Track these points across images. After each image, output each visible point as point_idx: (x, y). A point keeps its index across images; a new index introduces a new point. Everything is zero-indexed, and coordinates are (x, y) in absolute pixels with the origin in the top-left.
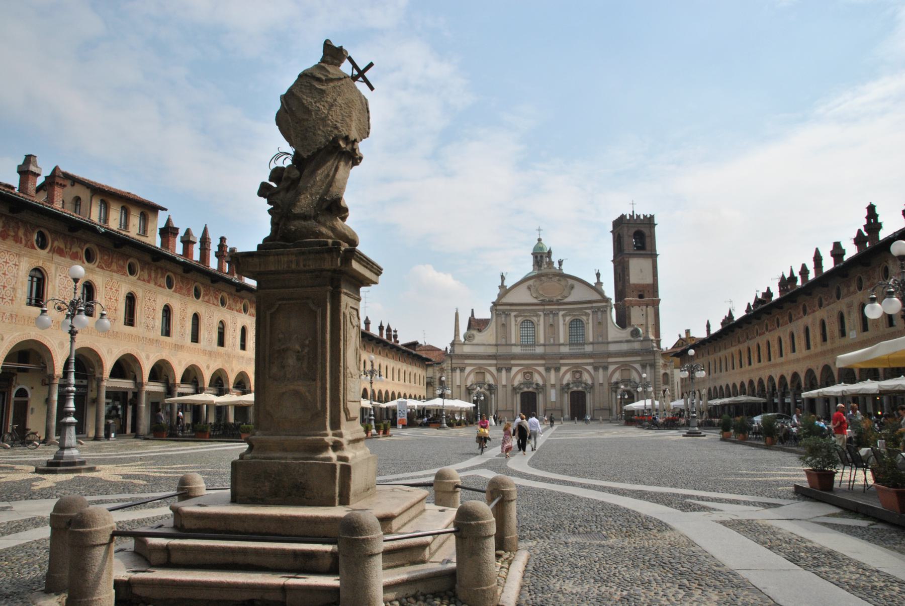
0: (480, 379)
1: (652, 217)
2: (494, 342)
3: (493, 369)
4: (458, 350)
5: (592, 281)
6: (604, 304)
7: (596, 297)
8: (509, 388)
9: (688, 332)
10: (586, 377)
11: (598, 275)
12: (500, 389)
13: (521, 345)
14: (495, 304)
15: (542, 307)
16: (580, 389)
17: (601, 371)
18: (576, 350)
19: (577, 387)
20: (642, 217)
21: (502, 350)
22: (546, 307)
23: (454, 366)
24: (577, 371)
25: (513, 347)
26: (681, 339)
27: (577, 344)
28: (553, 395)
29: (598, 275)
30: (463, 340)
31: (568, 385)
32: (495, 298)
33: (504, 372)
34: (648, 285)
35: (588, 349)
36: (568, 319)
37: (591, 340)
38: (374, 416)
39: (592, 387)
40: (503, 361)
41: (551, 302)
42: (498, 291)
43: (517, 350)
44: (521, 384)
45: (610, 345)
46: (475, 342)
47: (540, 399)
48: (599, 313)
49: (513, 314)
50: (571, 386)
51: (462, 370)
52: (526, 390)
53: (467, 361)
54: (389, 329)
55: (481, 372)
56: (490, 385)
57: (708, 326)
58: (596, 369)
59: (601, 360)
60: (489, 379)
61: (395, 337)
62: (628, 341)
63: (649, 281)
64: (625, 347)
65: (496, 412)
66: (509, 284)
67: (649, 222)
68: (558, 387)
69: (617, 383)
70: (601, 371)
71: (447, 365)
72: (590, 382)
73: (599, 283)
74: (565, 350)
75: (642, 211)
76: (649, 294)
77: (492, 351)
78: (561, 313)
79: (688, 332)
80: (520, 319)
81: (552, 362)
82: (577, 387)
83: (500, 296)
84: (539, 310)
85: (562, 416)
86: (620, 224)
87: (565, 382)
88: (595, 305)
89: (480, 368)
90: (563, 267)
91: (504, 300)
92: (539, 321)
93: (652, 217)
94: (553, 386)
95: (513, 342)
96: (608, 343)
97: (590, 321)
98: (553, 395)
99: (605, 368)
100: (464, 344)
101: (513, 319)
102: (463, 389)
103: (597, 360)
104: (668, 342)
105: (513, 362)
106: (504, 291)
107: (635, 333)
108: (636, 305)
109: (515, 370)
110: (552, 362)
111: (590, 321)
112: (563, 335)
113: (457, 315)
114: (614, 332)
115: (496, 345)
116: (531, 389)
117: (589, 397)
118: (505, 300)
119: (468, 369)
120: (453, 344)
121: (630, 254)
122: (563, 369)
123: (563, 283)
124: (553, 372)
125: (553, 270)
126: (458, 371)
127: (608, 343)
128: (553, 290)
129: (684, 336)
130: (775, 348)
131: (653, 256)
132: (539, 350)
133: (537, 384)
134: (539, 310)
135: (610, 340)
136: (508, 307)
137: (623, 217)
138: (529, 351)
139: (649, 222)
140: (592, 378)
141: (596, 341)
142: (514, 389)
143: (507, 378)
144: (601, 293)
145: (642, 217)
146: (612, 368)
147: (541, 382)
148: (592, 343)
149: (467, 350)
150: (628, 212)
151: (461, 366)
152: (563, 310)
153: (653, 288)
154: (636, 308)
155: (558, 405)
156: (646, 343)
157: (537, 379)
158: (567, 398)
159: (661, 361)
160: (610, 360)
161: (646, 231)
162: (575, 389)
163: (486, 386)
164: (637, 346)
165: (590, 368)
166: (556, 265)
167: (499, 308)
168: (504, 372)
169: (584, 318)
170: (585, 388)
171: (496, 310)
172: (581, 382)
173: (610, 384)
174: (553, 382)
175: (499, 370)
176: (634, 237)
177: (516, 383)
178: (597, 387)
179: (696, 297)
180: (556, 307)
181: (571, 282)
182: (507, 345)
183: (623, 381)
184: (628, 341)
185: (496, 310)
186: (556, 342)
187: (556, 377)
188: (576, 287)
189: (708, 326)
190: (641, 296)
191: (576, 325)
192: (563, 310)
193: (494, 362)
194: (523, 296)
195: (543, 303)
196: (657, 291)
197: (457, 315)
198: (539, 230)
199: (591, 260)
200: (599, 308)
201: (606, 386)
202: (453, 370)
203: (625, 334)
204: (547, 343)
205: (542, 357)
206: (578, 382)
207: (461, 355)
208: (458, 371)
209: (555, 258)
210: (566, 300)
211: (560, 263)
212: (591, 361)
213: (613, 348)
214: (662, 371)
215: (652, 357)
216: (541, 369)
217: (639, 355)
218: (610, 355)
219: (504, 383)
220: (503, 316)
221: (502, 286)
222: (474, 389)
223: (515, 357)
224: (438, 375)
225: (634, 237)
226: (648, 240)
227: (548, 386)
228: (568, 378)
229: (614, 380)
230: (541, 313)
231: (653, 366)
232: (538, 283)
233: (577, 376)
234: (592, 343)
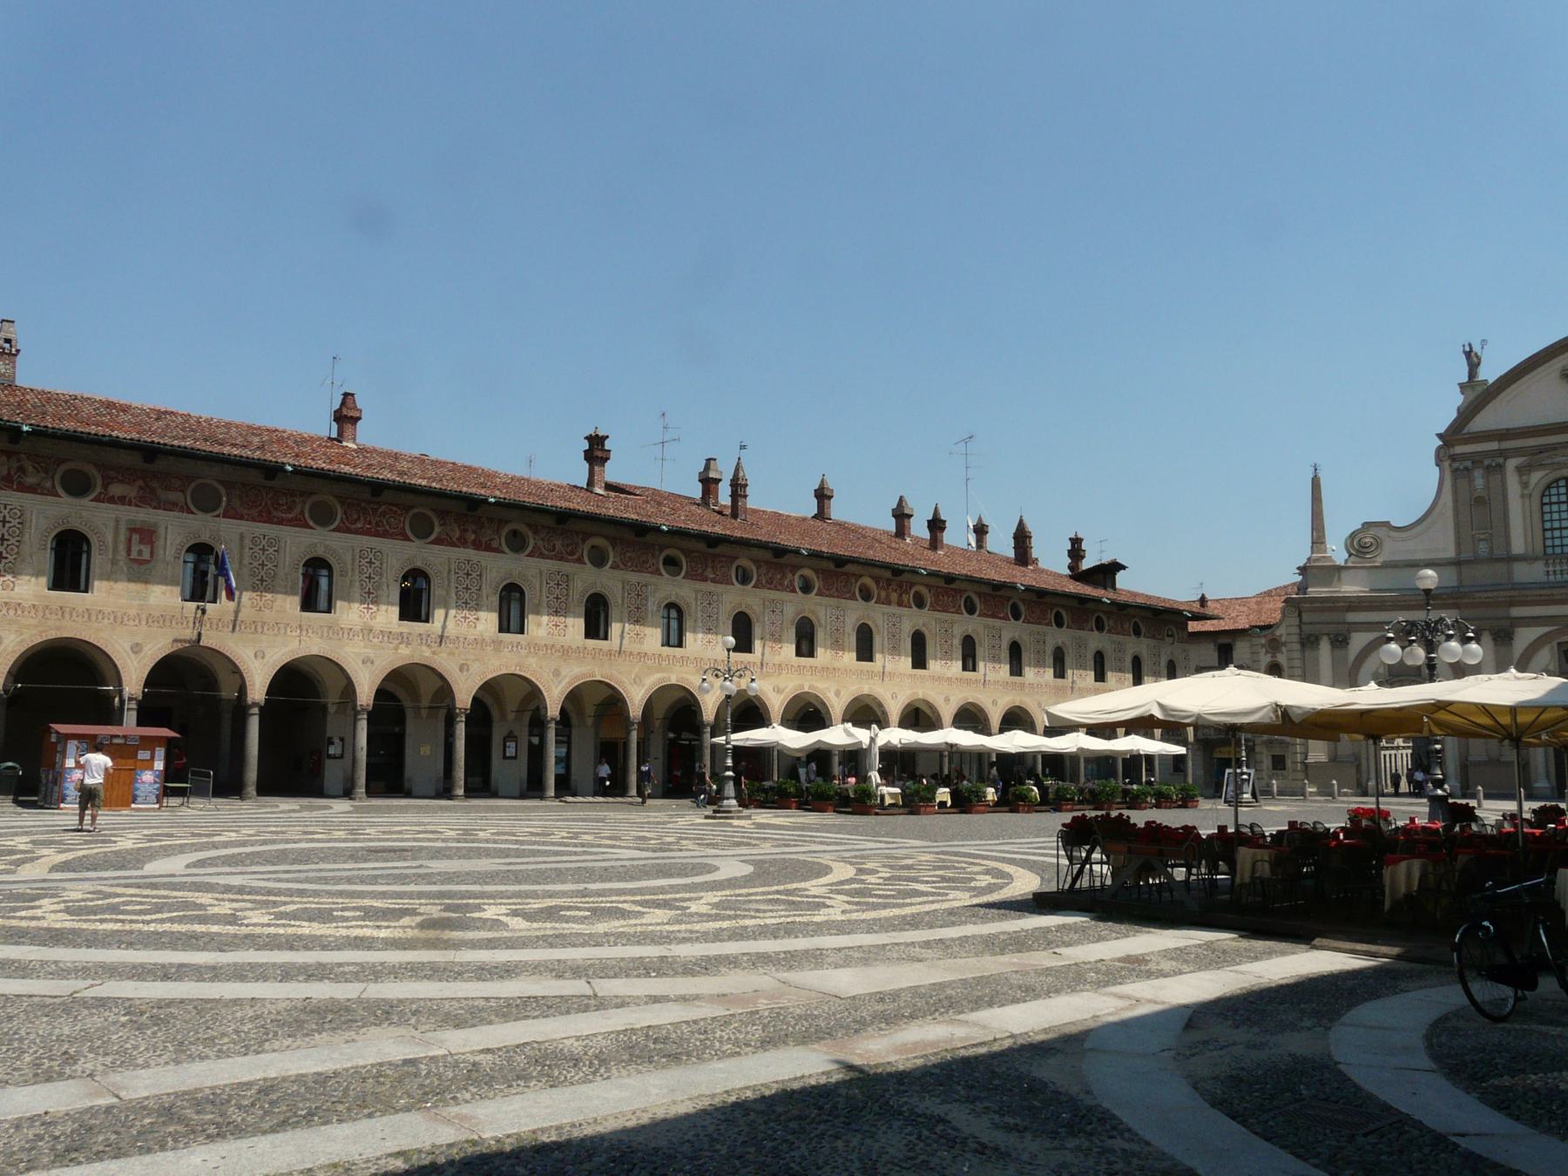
2: (1450, 553)
13: (1546, 557)
14: (1450, 437)
23: (1307, 629)
38: (733, 769)
42: (1458, 399)
51: (1340, 642)
53: (1352, 617)
66: (1490, 373)
80: (1536, 477)
83: (1466, 414)
105: (1516, 612)
106: (1479, 396)
113: (1316, 484)
115: (1457, 563)
118: (1485, 421)
126: (1325, 647)
136: (1494, 446)
167: (1459, 449)
171: (1453, 458)
182: (1493, 560)
185: (1453, 458)
197: (1316, 484)
220: (1478, 475)
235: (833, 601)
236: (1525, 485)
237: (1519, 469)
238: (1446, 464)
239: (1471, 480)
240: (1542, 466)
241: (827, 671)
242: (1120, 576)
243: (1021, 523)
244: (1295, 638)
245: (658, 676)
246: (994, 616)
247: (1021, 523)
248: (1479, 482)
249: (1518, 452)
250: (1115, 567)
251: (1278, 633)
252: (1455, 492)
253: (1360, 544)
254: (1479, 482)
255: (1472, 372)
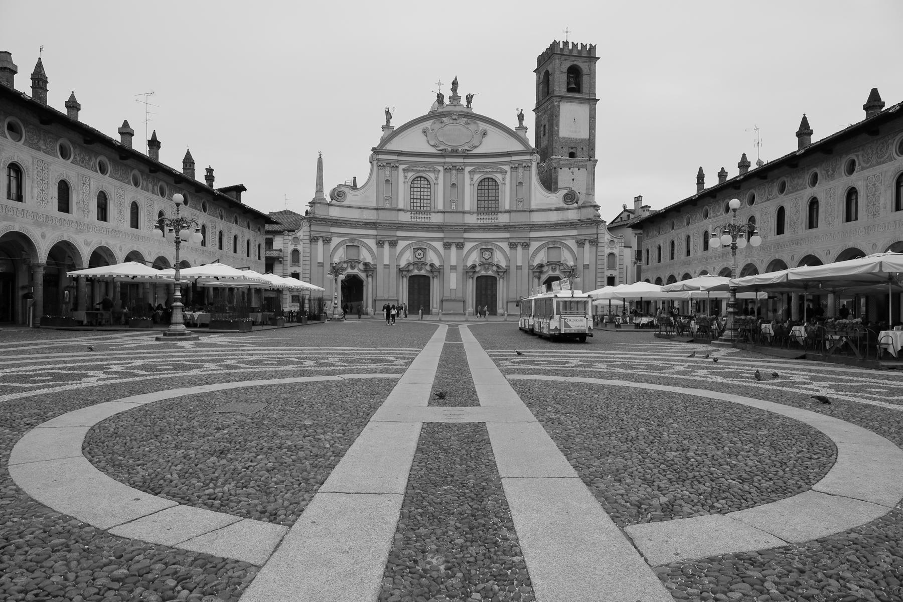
0: (352, 254)
1: (593, 48)
2: (374, 205)
3: (372, 243)
4: (320, 212)
5: (513, 124)
6: (528, 157)
7: (518, 147)
8: (393, 270)
9: (638, 199)
10: (499, 259)
11: (521, 117)
12: (380, 269)
13: (412, 211)
15: (442, 160)
16: (490, 273)
17: (519, 248)
18: (487, 220)
19: (486, 270)
20: (579, 48)
21: (385, 217)
22: (448, 160)
23: (313, 234)
24: (486, 248)
25: (401, 213)
26: (626, 210)
27: (488, 213)
28: (453, 280)
29: (521, 117)
30: (328, 199)
31: (474, 267)
32: (376, 144)
33: (387, 246)
34: (583, 140)
35: (503, 219)
36: (477, 177)
37: (507, 207)
39: (506, 272)
40: (386, 231)
41: (454, 153)
43: (405, 217)
44: (409, 264)
45: (533, 214)
46: (346, 203)
47: (435, 285)
48: (520, 170)
49: (402, 167)
50: (478, 269)
51: (327, 241)
52: (416, 272)
53: (333, 230)
54: (188, 161)
55: (353, 245)
56: (366, 264)
57: (701, 177)
58: (513, 246)
59: (520, 233)
60: (365, 256)
61: (210, 177)
62: (558, 209)
63: (585, 135)
64: (554, 217)
65: (375, 301)
66: (396, 123)
67: (590, 55)
68: (460, 269)
69: (541, 266)
70: (519, 248)
71: (303, 233)
72: (503, 264)
73: (522, 127)
74: (471, 219)
75: (579, 37)
76: (583, 153)
77: (370, 216)
78: (468, 169)
79: (638, 199)
80: (411, 175)
81: (453, 234)
82: (486, 270)
84: (438, 164)
85: (465, 309)
86: (550, 56)
87: (469, 263)
88: (514, 158)
89: (353, 240)
90: (472, 105)
91: (390, 147)
92: (437, 179)
93: (593, 48)
94: (453, 268)
95: (401, 206)
96: (531, 211)
97: (508, 181)
98: (453, 280)
99: (526, 246)
100: (330, 205)
101: (401, 173)
102: (327, 268)
103: (515, 235)
104: (608, 215)
105: (399, 233)
106: (391, 134)
107: (570, 197)
108: (566, 166)
109: (402, 244)
110: (453, 234)
111: (508, 181)
112: (469, 200)
114: (539, 196)
115: (377, 209)
116: (423, 272)
117: (501, 285)
118: (392, 146)
119: (335, 241)
120: (312, 204)
121: (562, 97)
122: (468, 246)
123: (472, 127)
124: (453, 249)
125: (458, 109)
126: (320, 243)
127: (531, 211)
128: (456, 134)
129: (631, 206)
130: (680, 247)
131: (592, 101)
132: (436, 219)
133: (432, 265)
134: (438, 164)
135: (533, 207)
136: (395, 157)
137: (555, 44)
138: (421, 219)
139: (590, 55)
140: (508, 259)
141: (514, 207)
142: (401, 270)
143: (391, 256)
144: (524, 142)
145: (579, 48)
146: (534, 245)
147: (437, 263)
148: (509, 212)
149: (335, 213)
150: (561, 39)
151: (324, 235)
152: (471, 164)
153: (590, 144)
154: (566, 169)
155: (459, 294)
156: (584, 211)
157: (432, 258)
158: (471, 285)
159: (606, 236)
160: (533, 234)
161: (583, 66)
162: (483, 273)
163: (361, 267)
164: (572, 215)
165: (505, 245)
166: (463, 102)
167: (381, 157)
168: (387, 246)
169: (499, 177)
170: (498, 273)
172: (491, 264)
173: (531, 267)
174: (453, 263)
175: (380, 244)
176: (567, 74)
177: (403, 264)
178: (513, 269)
179: (643, 159)
180: (461, 160)
181: (483, 126)
183: (549, 264)
184: (558, 209)
186: (460, 209)
187: (458, 256)
188: (489, 132)
189: (701, 177)
190: (572, 155)
191: (488, 187)
192: (471, 164)
193: (374, 232)
194: (414, 142)
195: (443, 154)
196: (593, 149)
198: (440, 84)
199: (509, 97)
200: (520, 163)
201: (526, 270)
202: (313, 240)
203: (556, 199)
204: (447, 209)
205: (440, 228)
206: (486, 264)
207: (325, 220)
208: (320, 243)
209: (462, 92)
210: (476, 151)
211: (469, 99)
212: (507, 235)
213: (537, 218)
214: (608, 251)
215: (594, 231)
216: (439, 245)
217: (575, 228)
218: (533, 227)
219: (386, 262)
220: (388, 169)
221: (386, 127)
222: (344, 270)
223: (402, 226)
224: (291, 248)
225: (567, 74)
226: (585, 79)
227: (447, 269)
228: (474, 258)
229: (536, 262)
230: (441, 168)
231: (595, 242)
232: (438, 125)
233: (487, 255)
234: (509, 212)
235: (118, 183)
236: (472, 179)
237: (404, 170)
238: (375, 162)
239: (385, 172)
240: (413, 171)
241: (115, 232)
242: (243, 193)
243: (188, 153)
244: (308, 237)
245: (5, 223)
246: (195, 208)
247: (188, 153)
248: (388, 173)
249: (405, 162)
250: (240, 189)
251: (298, 235)
252: (378, 176)
253: (338, 194)
254: (388, 173)
255: (388, 121)
